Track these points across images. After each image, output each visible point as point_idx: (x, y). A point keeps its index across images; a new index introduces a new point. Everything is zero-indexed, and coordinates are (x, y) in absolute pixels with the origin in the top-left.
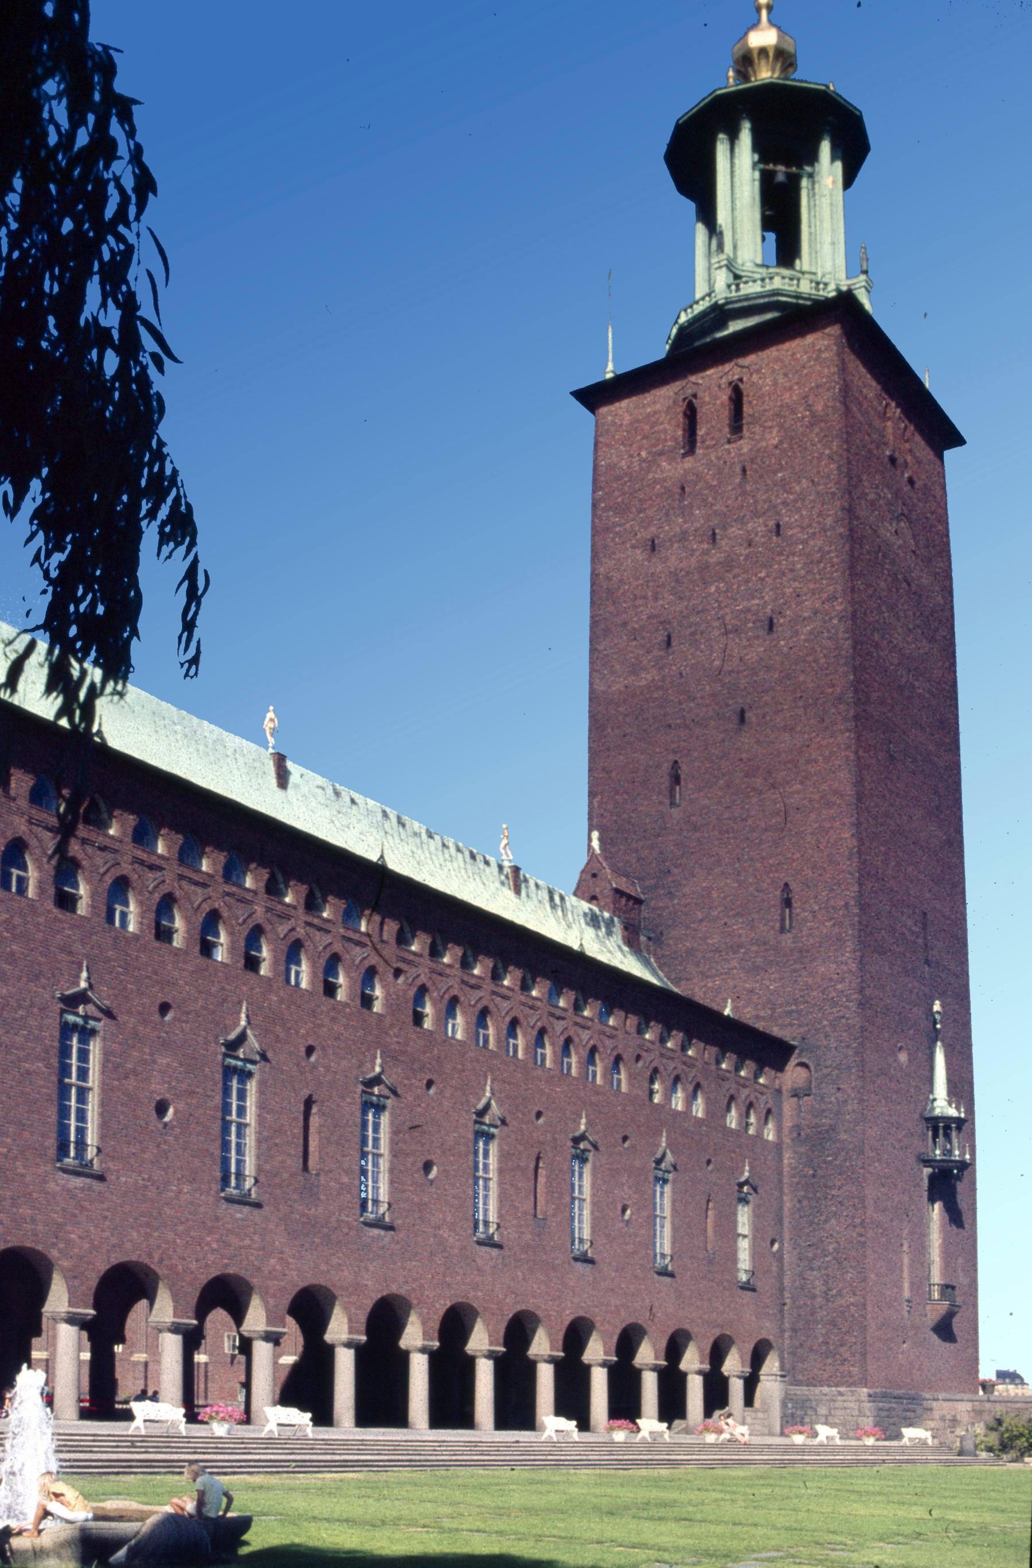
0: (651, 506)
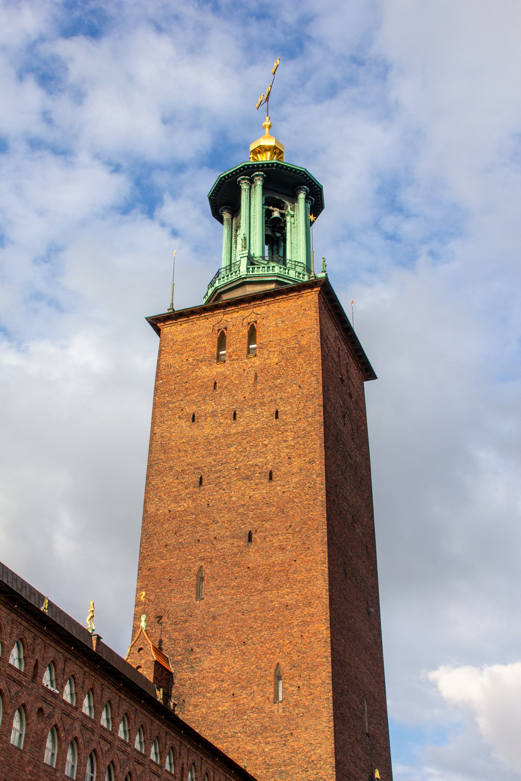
0: (193, 394)
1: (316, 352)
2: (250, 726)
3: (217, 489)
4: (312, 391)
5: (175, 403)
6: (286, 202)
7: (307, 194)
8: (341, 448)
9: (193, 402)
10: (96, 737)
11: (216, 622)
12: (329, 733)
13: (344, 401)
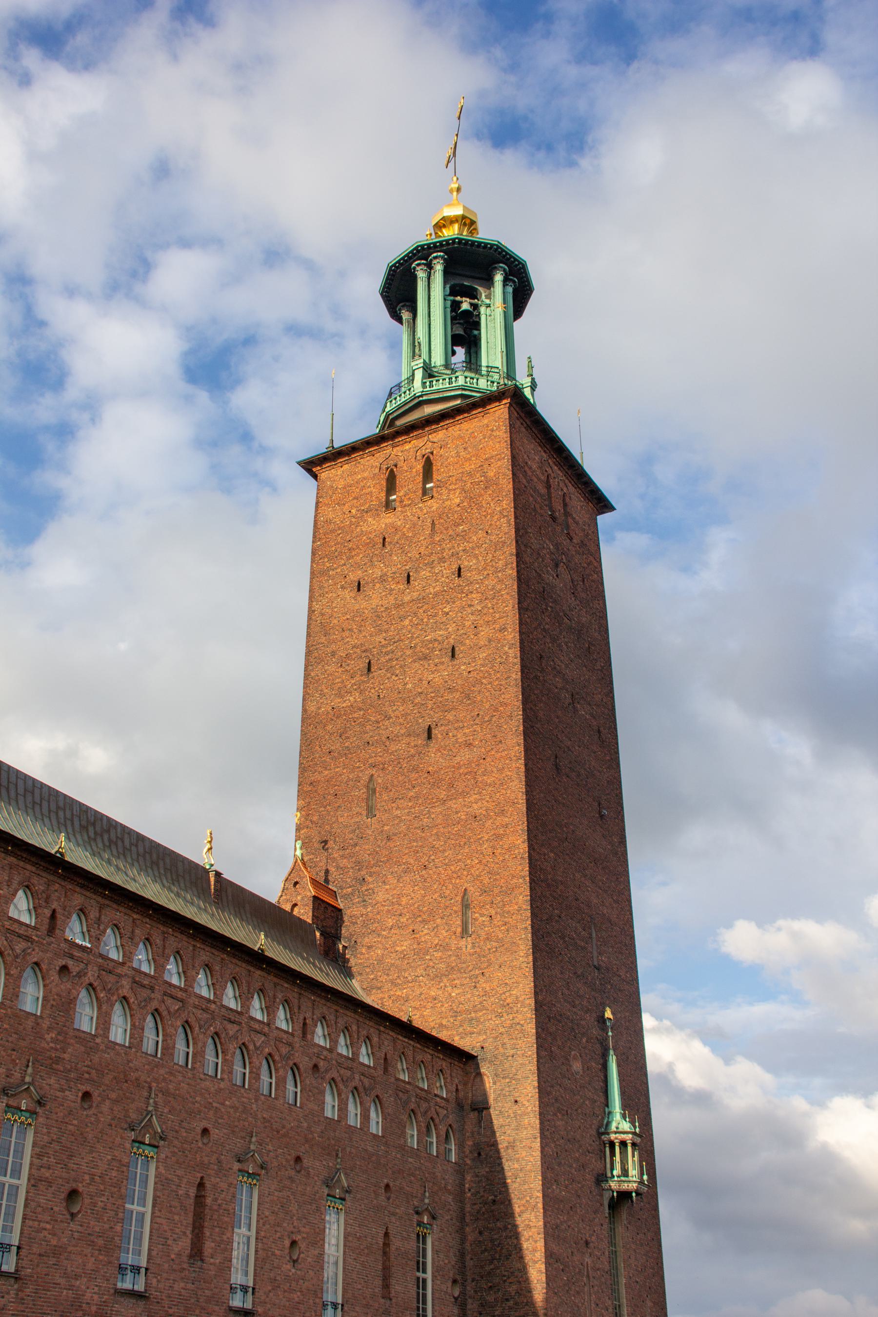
0: (357, 555)
1: (507, 485)
2: (433, 967)
3: (389, 675)
4: (502, 538)
5: (336, 569)
6: (479, 288)
7: (506, 274)
8: (551, 607)
9: (358, 566)
10: (157, 995)
11: (391, 844)
12: (527, 970)
13: (557, 546)
